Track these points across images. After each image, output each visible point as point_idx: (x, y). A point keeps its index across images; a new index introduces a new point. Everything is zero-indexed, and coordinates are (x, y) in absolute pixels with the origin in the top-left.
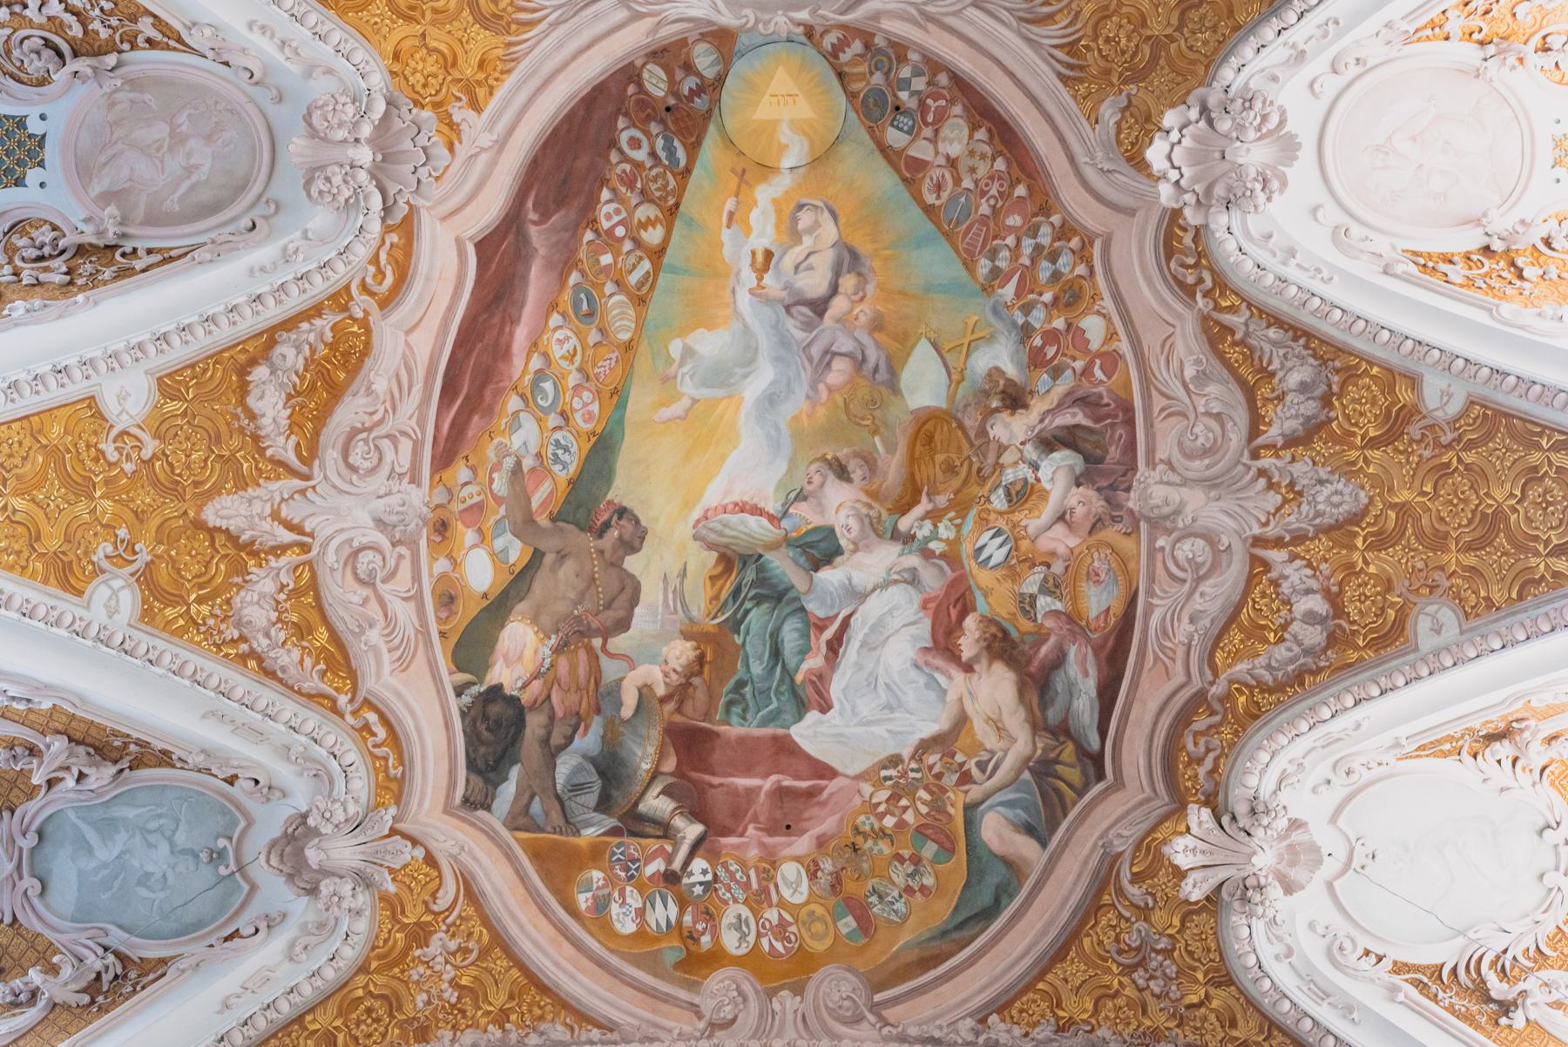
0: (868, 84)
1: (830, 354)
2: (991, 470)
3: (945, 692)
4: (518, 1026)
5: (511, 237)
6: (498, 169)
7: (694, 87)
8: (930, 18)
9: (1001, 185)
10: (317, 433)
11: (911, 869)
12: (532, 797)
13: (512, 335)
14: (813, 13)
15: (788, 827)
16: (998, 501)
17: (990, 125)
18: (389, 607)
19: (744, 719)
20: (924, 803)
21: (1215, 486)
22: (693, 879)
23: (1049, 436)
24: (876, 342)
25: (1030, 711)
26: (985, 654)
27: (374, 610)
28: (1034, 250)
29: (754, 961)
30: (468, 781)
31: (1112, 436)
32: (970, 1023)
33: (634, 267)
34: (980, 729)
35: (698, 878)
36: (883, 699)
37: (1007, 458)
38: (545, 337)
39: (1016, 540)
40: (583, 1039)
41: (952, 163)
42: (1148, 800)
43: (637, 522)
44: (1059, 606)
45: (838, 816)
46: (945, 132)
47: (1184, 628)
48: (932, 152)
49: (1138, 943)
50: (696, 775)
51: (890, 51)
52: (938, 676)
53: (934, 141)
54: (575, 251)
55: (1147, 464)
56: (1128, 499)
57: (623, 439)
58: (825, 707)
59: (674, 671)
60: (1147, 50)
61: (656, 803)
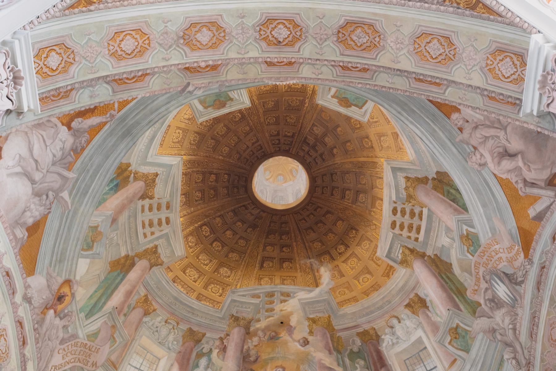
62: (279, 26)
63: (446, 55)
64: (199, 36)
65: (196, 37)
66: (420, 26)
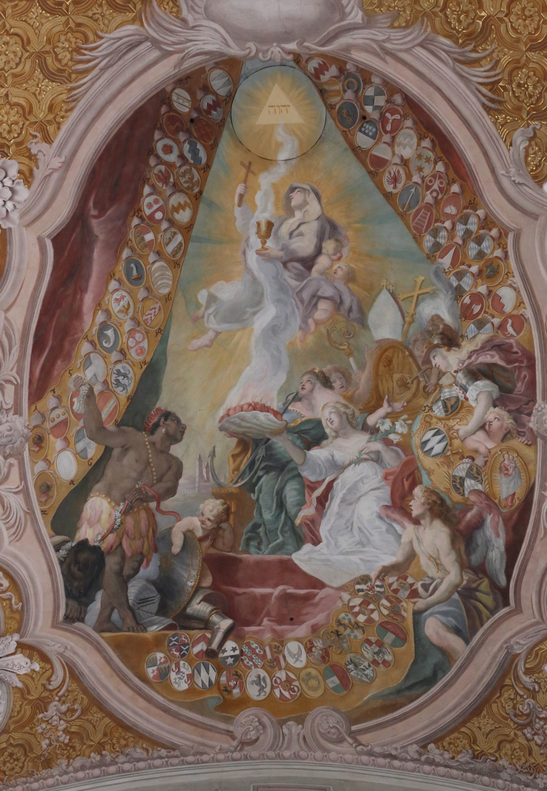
0: (342, 98)
1: (316, 298)
2: (433, 388)
4: (111, 752)
5: (78, 230)
6: (66, 183)
7: (211, 103)
8: (388, 53)
9: (441, 183)
11: (377, 649)
12: (112, 610)
13: (82, 300)
14: (300, 44)
15: (292, 619)
16: (438, 410)
17: (433, 137)
18: (5, 500)
19: (259, 549)
20: (386, 608)
22: (226, 654)
23: (474, 368)
25: (459, 555)
26: (428, 513)
28: (465, 233)
30: (67, 605)
31: (519, 376)
33: (170, 240)
34: (424, 561)
35: (229, 653)
36: (357, 538)
37: (444, 381)
38: (106, 299)
39: (451, 440)
40: (155, 755)
41: (405, 162)
42: (537, 623)
43: (178, 421)
44: (480, 487)
45: (326, 613)
46: (400, 139)
48: (390, 154)
49: (528, 711)
50: (225, 588)
51: (358, 75)
53: (392, 144)
54: (126, 234)
56: (529, 421)
57: (166, 364)
58: (316, 541)
59: (209, 519)
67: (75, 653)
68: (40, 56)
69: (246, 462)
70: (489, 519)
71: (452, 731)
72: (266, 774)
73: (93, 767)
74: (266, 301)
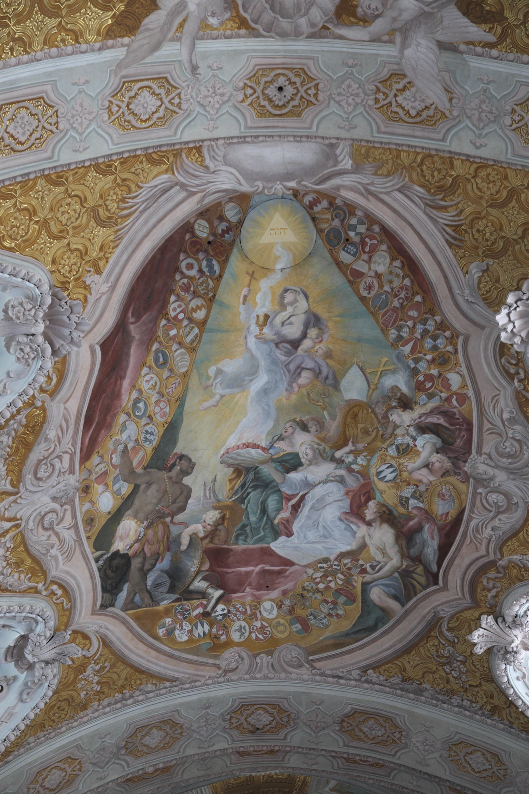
0: (330, 225)
1: (300, 369)
2: (389, 436)
3: (355, 533)
4: (130, 690)
5: (120, 335)
6: (112, 301)
7: (225, 228)
9: (407, 293)
10: (21, 470)
11: (332, 606)
12: (135, 595)
13: (121, 385)
14: (299, 183)
16: (392, 451)
17: (402, 259)
18: (61, 535)
19: (246, 541)
20: (341, 580)
21: (512, 473)
22: (217, 614)
23: (423, 425)
24: (327, 364)
25: (401, 547)
26: (379, 519)
27: (54, 540)
28: (423, 331)
29: (248, 644)
30: (103, 597)
32: (358, 671)
33: (189, 333)
34: (373, 550)
36: (322, 532)
37: (398, 432)
38: (139, 381)
39: (400, 472)
40: (161, 687)
41: (378, 276)
43: (190, 460)
44: (421, 505)
45: (294, 582)
46: (375, 258)
47: (488, 532)
48: (367, 269)
49: (448, 655)
51: (345, 208)
52: (352, 525)
53: (369, 261)
55: (477, 453)
56: (465, 466)
57: (182, 422)
58: (290, 534)
59: (209, 525)
60: (501, 244)
61: (199, 584)
62: (258, 712)
63: (494, 772)
64: (147, 740)
65: (143, 741)
66: (457, 733)
67: (107, 629)
68: (94, 210)
69: (239, 483)
70: (426, 527)
71: (387, 663)
72: (242, 690)
73: (116, 703)
74: (260, 371)
